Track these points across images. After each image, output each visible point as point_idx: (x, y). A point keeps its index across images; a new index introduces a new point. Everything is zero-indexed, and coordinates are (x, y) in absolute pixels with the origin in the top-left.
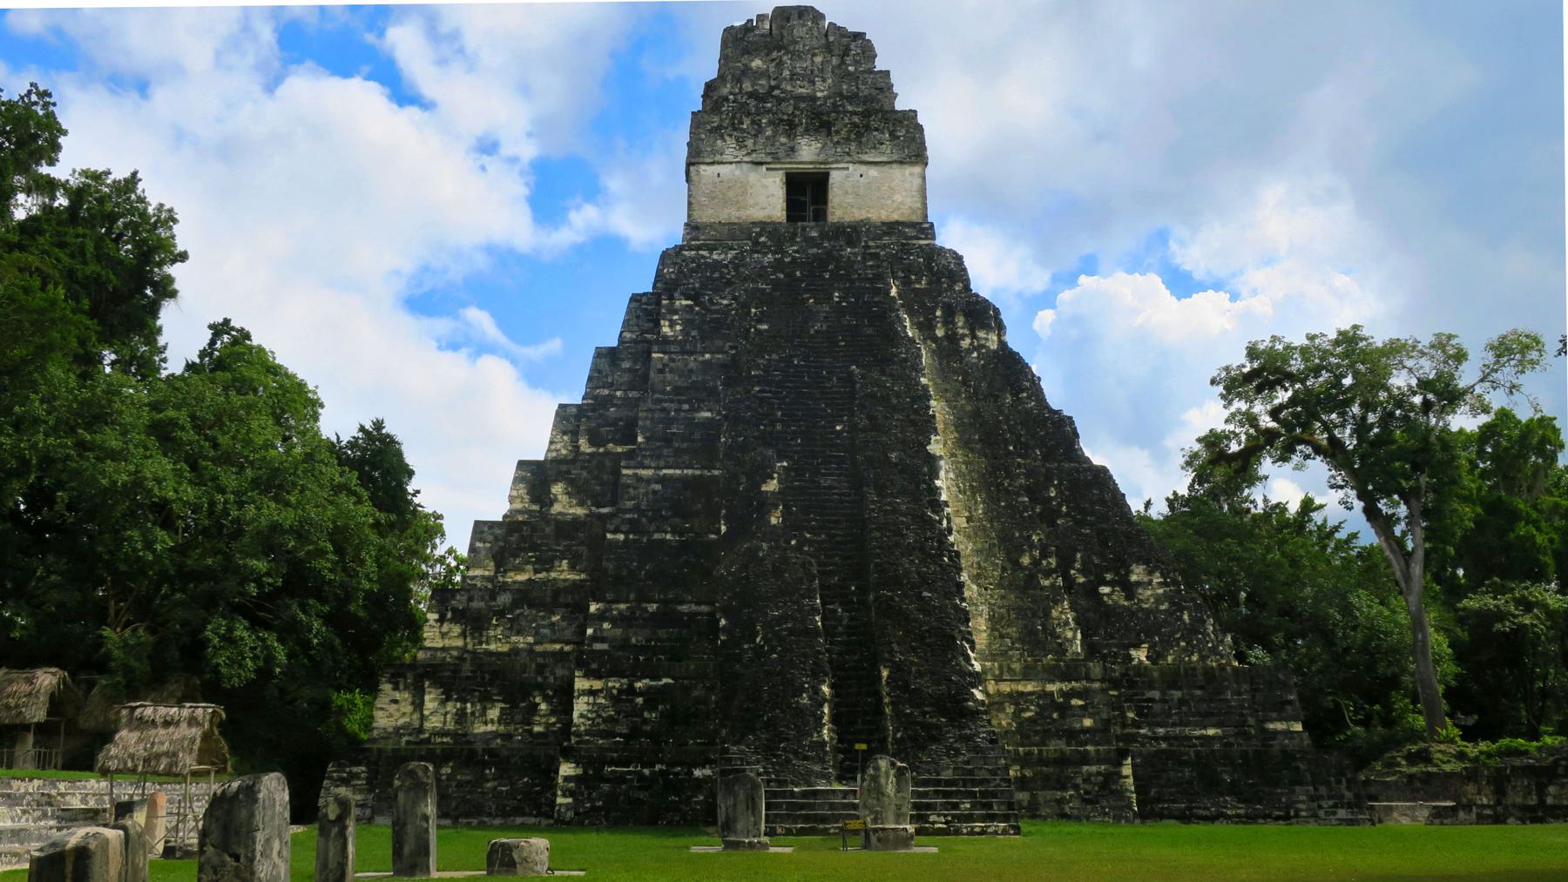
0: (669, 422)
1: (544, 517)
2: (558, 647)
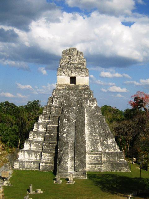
0: (54, 118)
1: (38, 130)
2: (40, 148)
